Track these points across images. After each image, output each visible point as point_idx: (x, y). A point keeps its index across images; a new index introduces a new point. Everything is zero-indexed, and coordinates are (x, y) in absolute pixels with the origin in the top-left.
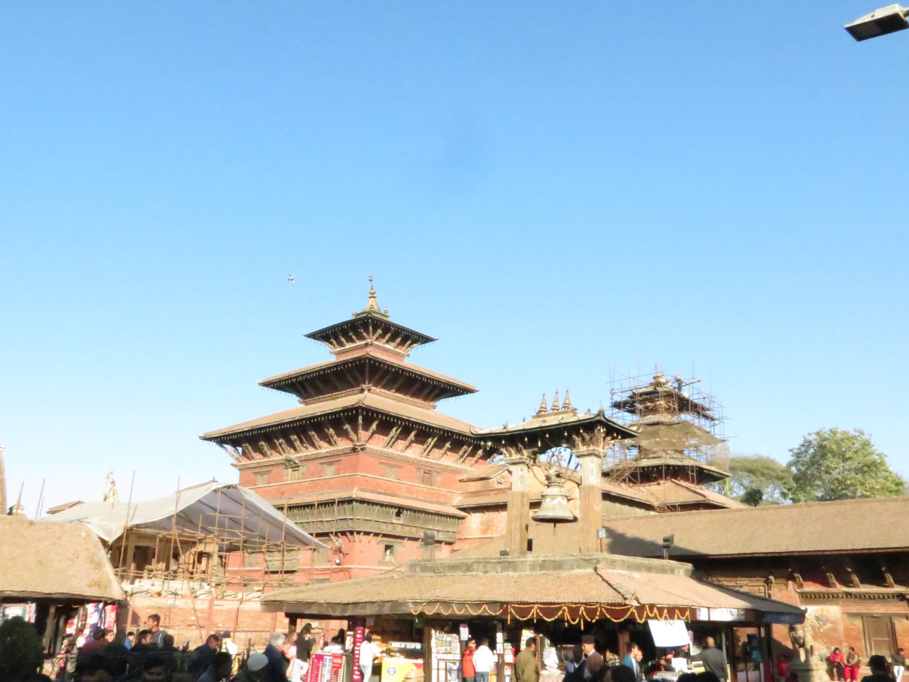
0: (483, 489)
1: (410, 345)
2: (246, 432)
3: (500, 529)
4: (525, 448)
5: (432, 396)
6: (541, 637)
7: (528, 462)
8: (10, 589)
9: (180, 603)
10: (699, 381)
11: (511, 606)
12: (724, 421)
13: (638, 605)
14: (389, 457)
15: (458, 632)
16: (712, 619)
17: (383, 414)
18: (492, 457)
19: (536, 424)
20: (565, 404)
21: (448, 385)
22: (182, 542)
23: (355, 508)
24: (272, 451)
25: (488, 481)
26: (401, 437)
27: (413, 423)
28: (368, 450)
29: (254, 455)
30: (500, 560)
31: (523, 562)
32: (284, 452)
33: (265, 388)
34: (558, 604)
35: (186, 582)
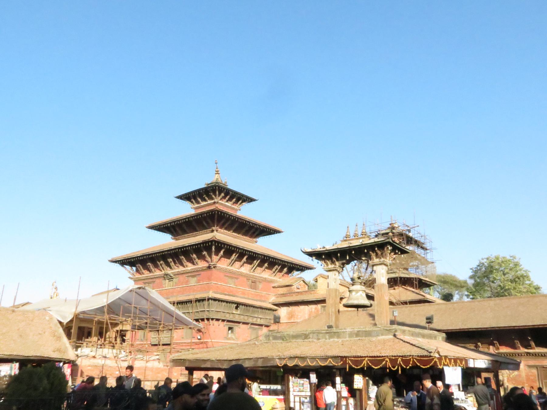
0: (288, 292)
1: (241, 203)
2: (139, 257)
3: (299, 317)
4: (338, 260)
5: (255, 234)
6: (367, 379)
7: (339, 269)
8: (2, 353)
9: (108, 362)
10: (418, 226)
11: (349, 359)
12: (433, 250)
13: (439, 356)
14: (231, 272)
15: (309, 378)
16: (476, 366)
17: (228, 245)
18: (292, 273)
19: (345, 245)
20: (363, 232)
21: (265, 228)
22: (111, 324)
23: (210, 303)
24: (155, 269)
25: (291, 287)
26: (237, 259)
27: (246, 250)
28: (218, 267)
29: (144, 271)
30: (327, 331)
31: (344, 332)
32: (163, 269)
33: (150, 230)
34: (383, 357)
35: (110, 350)
